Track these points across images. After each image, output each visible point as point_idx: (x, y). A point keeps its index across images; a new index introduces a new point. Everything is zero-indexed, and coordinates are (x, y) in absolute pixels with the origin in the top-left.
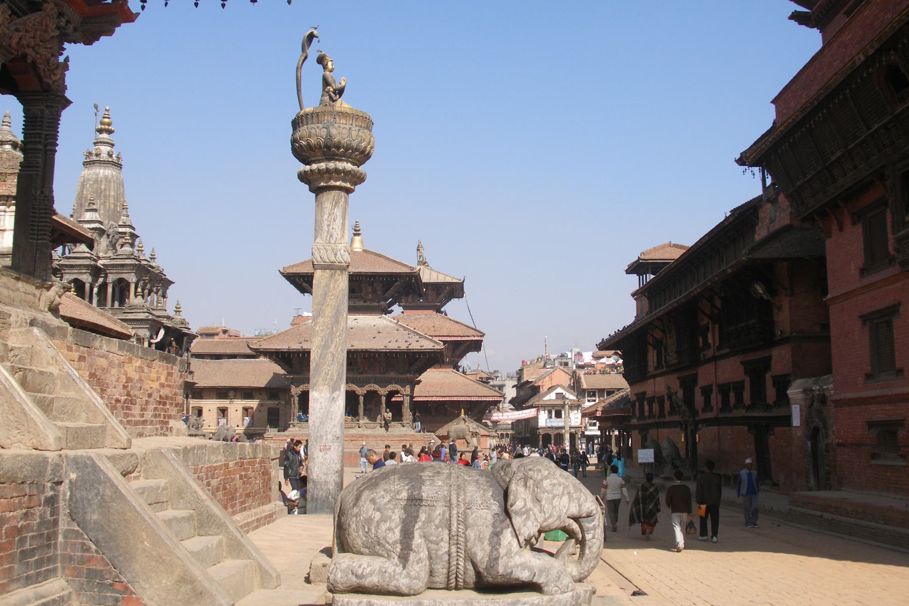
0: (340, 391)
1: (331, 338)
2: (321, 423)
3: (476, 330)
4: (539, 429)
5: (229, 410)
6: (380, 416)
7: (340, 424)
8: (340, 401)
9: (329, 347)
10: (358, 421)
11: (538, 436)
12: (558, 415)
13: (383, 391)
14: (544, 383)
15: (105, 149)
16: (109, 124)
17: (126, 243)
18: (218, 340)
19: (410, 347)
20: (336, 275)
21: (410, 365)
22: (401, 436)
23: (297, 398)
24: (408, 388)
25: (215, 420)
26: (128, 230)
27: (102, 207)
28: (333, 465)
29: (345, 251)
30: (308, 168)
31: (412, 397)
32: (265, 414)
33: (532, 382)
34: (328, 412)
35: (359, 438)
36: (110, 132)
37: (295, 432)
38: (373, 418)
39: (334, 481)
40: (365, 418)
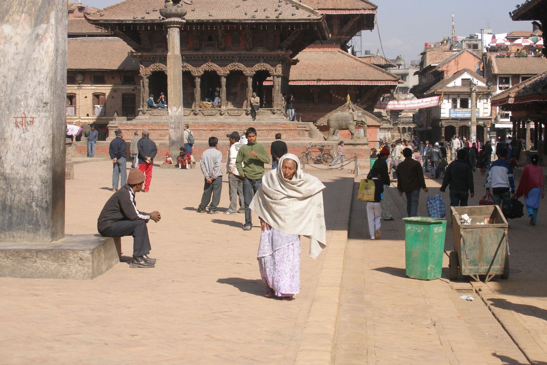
0: (48, 22)
2: (16, 78)
4: (441, 120)
5: (77, 96)
6: (246, 101)
7: (48, 80)
8: (49, 40)
10: (220, 107)
11: (441, 128)
12: (464, 104)
13: (249, 72)
14: (449, 68)
18: (73, 18)
19: (281, 17)
21: (282, 39)
22: (270, 126)
23: (147, 80)
24: (279, 69)
28: (39, 150)
31: (285, 78)
32: (119, 101)
33: (435, 67)
34: (29, 60)
35: (220, 127)
37: (144, 121)
38: (238, 104)
39: (40, 176)
40: (229, 103)
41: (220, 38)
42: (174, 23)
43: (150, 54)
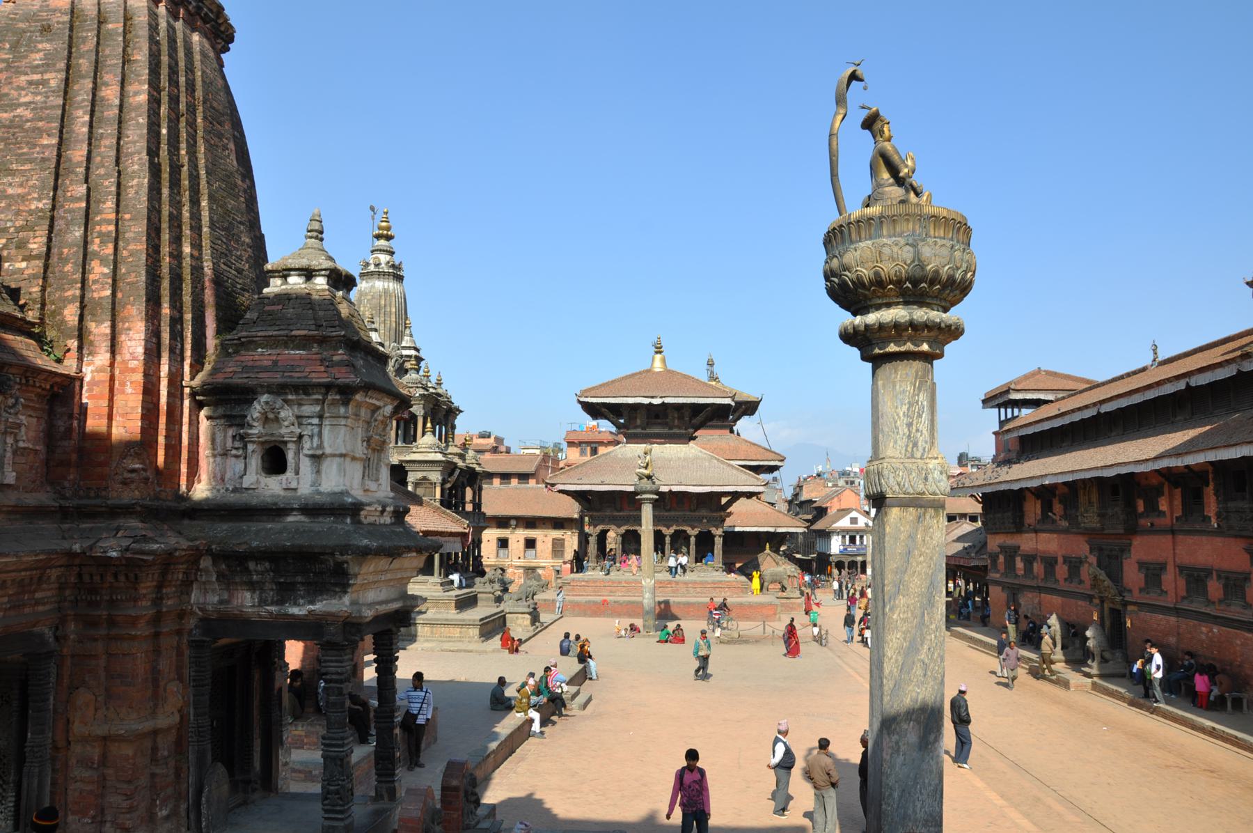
1: (922, 634)
3: (770, 451)
4: (830, 555)
9: (918, 651)
15: (384, 258)
16: (389, 229)
17: (411, 369)
20: (928, 517)
22: (715, 584)
25: (495, 552)
26: (413, 353)
27: (383, 325)
29: (941, 473)
30: (858, 320)
33: (815, 502)
36: (389, 238)
41: (666, 501)
42: (647, 499)
43: (598, 514)
